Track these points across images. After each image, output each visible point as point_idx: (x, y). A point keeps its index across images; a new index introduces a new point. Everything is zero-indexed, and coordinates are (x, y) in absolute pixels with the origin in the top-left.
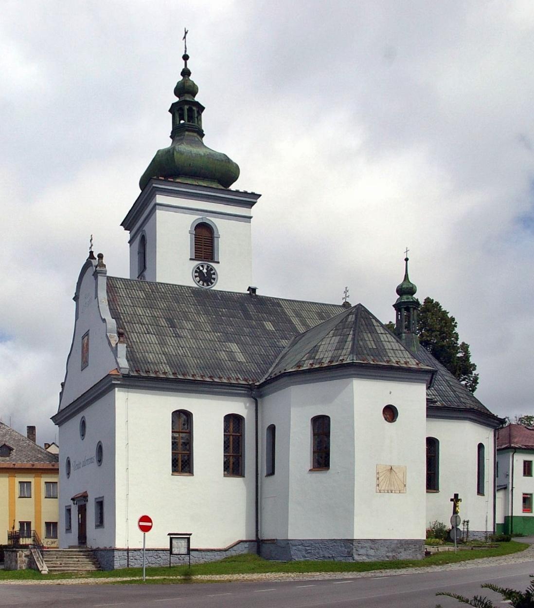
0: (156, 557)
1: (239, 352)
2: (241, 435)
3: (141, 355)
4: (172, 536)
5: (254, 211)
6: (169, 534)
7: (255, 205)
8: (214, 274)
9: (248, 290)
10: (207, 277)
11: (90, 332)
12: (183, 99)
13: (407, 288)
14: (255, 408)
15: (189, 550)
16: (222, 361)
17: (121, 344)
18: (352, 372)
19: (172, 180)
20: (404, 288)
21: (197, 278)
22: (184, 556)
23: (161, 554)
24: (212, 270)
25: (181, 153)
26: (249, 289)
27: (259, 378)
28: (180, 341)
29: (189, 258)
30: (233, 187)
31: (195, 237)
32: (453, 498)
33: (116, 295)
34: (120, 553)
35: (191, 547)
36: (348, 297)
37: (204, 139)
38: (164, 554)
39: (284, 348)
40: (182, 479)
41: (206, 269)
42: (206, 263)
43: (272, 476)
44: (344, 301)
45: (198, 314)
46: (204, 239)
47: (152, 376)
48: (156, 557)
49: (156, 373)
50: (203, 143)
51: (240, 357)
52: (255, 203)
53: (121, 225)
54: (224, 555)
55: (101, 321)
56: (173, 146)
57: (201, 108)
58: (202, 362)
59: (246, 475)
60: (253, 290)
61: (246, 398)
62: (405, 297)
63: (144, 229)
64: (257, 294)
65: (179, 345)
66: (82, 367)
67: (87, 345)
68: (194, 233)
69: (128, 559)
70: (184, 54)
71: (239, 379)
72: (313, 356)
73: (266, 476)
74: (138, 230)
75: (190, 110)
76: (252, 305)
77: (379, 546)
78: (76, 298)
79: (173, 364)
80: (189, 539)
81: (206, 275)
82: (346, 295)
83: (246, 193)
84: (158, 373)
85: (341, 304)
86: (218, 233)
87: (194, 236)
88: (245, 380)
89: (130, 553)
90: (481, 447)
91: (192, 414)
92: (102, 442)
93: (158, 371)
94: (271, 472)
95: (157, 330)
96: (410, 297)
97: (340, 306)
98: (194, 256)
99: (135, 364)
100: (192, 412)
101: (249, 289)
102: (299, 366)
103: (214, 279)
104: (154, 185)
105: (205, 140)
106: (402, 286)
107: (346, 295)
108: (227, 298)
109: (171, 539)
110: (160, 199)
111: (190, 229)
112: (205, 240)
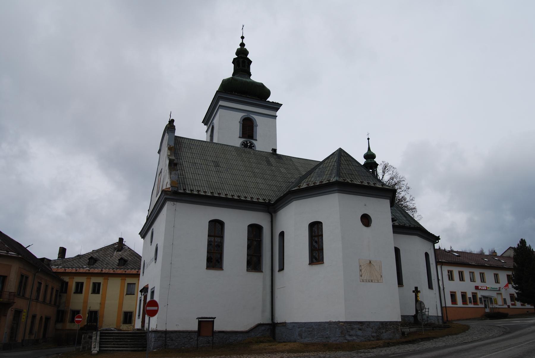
2: (261, 240)
4: (200, 320)
5: (278, 113)
8: (254, 146)
9: (272, 150)
13: (370, 155)
24: (252, 144)
29: (239, 136)
33: (182, 146)
39: (293, 183)
40: (214, 273)
42: (249, 140)
43: (283, 271)
53: (202, 123)
62: (369, 160)
68: (242, 123)
70: (242, 36)
71: (259, 199)
73: (279, 271)
74: (211, 123)
79: (212, 187)
84: (200, 192)
86: (257, 123)
87: (242, 125)
90: (427, 255)
93: (200, 191)
96: (372, 160)
98: (242, 135)
111: (239, 120)
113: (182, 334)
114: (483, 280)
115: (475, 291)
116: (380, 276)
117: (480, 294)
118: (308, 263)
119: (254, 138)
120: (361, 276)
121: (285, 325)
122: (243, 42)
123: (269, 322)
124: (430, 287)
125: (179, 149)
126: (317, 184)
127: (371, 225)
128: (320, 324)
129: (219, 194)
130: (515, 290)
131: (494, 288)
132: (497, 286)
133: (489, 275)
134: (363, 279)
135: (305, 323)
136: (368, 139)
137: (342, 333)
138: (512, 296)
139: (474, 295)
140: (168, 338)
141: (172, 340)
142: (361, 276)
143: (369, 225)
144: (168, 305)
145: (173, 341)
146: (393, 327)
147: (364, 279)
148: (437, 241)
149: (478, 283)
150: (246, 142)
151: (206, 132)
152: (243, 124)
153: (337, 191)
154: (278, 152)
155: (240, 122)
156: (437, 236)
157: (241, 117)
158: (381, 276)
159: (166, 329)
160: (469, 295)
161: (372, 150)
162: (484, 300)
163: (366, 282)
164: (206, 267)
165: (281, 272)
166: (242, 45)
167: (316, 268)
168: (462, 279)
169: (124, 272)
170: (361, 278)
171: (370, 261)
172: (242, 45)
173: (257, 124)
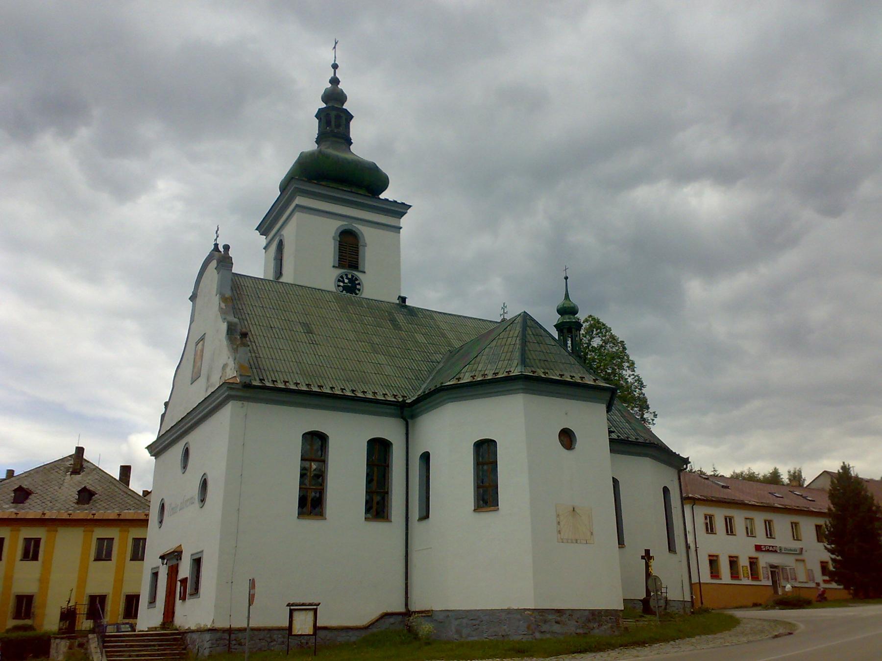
3: (268, 362)
4: (292, 607)
5: (404, 221)
6: (289, 605)
7: (406, 215)
8: (359, 284)
9: (398, 299)
10: (352, 287)
11: (206, 335)
12: (330, 104)
15: (316, 628)
20: (565, 307)
22: (308, 637)
24: (356, 279)
29: (332, 265)
30: (382, 196)
37: (351, 147)
39: (439, 363)
42: (352, 273)
43: (427, 520)
44: (502, 317)
46: (349, 246)
47: (280, 386)
49: (285, 384)
50: (350, 149)
52: (406, 213)
54: (364, 634)
56: (319, 148)
61: (393, 419)
62: (567, 316)
64: (407, 304)
65: (316, 354)
67: (202, 351)
69: (230, 643)
71: (386, 394)
73: (418, 520)
74: (275, 235)
75: (338, 117)
76: (401, 315)
77: (567, 620)
78: (193, 298)
80: (315, 611)
82: (504, 311)
87: (338, 243)
88: (395, 396)
89: (232, 635)
90: (666, 491)
93: (288, 382)
96: (572, 317)
98: (337, 263)
103: (359, 290)
107: (504, 311)
108: (374, 306)
109: (291, 611)
113: (256, 633)
114: (770, 534)
115: (755, 554)
116: (589, 534)
117: (765, 560)
118: (473, 509)
119: (360, 268)
120: (559, 532)
121: (431, 615)
122: (337, 75)
123: (402, 609)
124: (671, 548)
126: (489, 378)
127: (576, 447)
128: (493, 612)
129: (320, 387)
130: (829, 554)
131: (791, 550)
132: (796, 545)
133: (782, 524)
134: (562, 538)
135: (468, 611)
136: (566, 278)
137: (528, 627)
138: (824, 566)
139: (753, 562)
140: (233, 641)
141: (240, 644)
142: (559, 532)
143: (572, 447)
144: (232, 582)
145: (242, 645)
146: (610, 619)
147: (564, 538)
148: (685, 466)
149: (761, 539)
150: (346, 275)
151: (264, 248)
152: (339, 242)
153: (521, 391)
155: (334, 238)
156: (686, 457)
157: (337, 229)
158: (592, 533)
159: (230, 626)
160: (744, 562)
161: (575, 300)
162: (771, 571)
163: (568, 542)
164: (297, 515)
165: (424, 522)
166: (335, 81)
167: (487, 517)
168: (730, 530)
169: (90, 517)
170: (559, 535)
171: (574, 508)
172: (335, 81)
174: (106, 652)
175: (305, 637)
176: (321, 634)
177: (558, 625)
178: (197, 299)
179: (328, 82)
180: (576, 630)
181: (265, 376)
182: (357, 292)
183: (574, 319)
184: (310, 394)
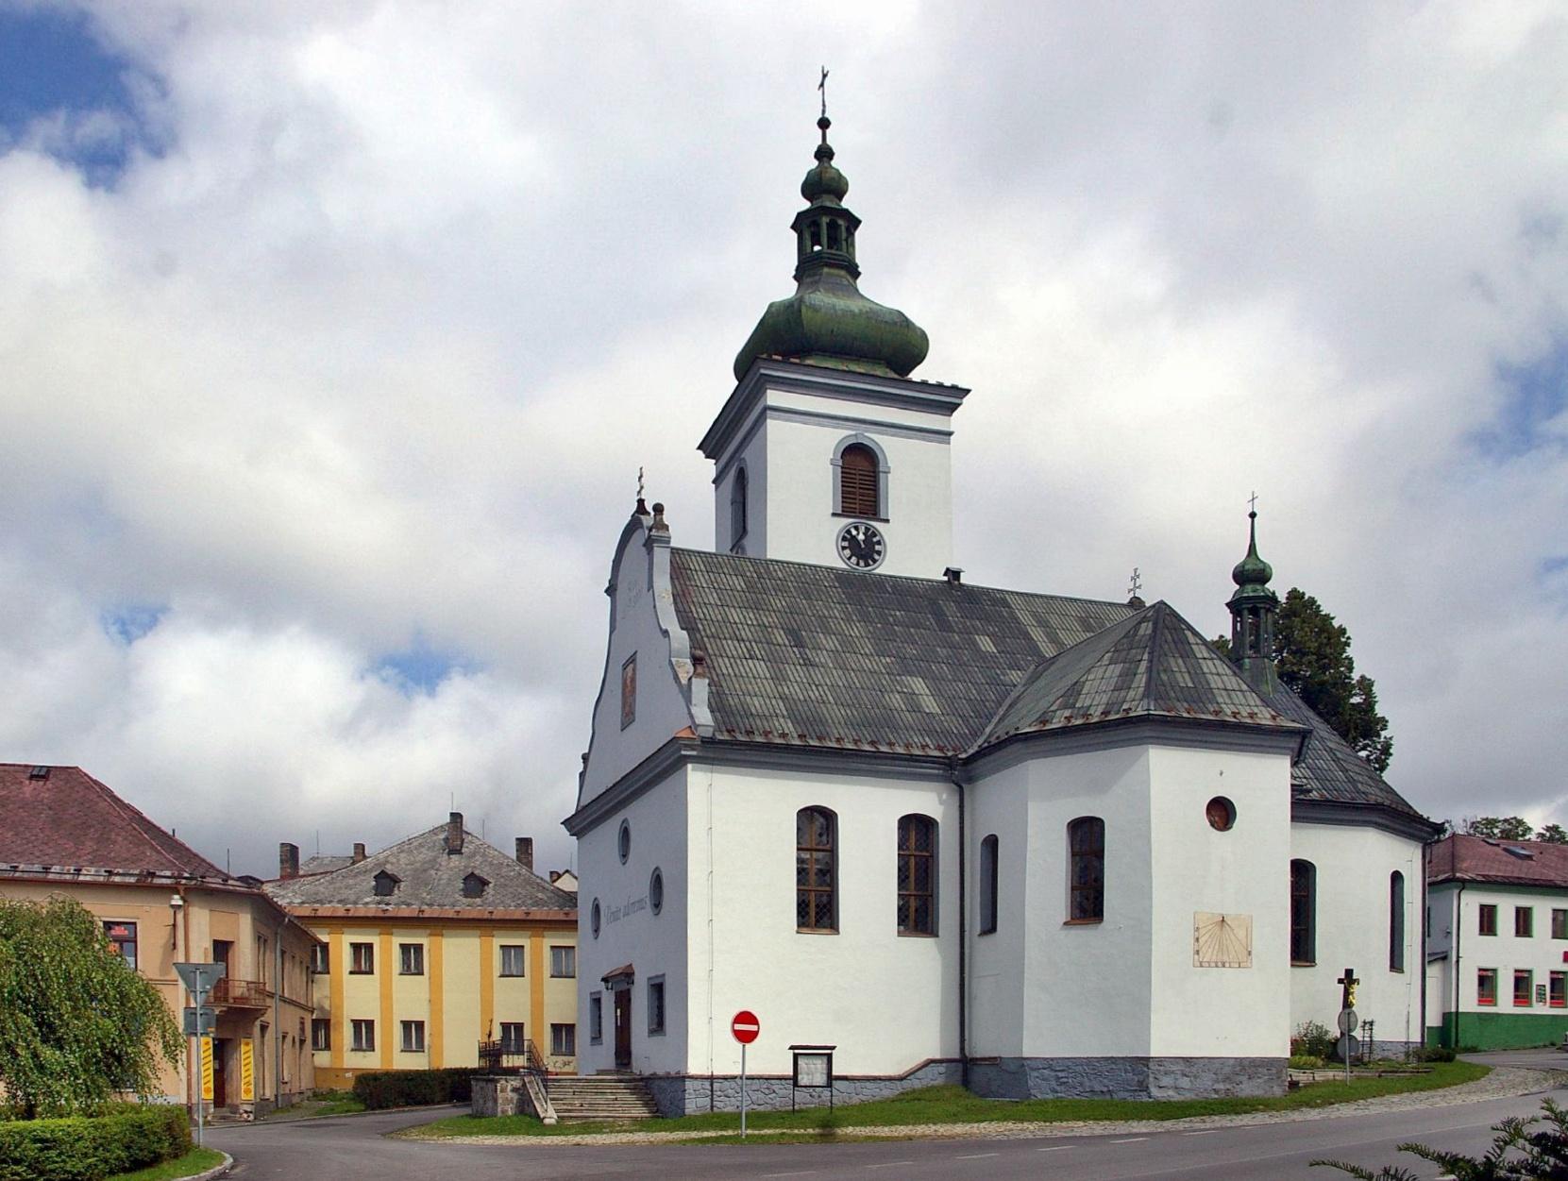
0: (767, 1091)
1: (927, 695)
2: (932, 856)
3: (737, 701)
4: (797, 1051)
5: (956, 421)
6: (792, 1048)
7: (960, 409)
8: (879, 543)
9: (945, 574)
10: (865, 549)
11: (638, 655)
12: (818, 203)
13: (1254, 570)
14: (958, 804)
15: (831, 1078)
16: (895, 712)
17: (698, 679)
18: (1148, 734)
19: (797, 361)
20: (1248, 570)
21: (845, 552)
22: (821, 1089)
23: (776, 1085)
24: (874, 535)
25: (815, 309)
26: (947, 572)
27: (967, 744)
28: (812, 673)
29: (831, 511)
30: (916, 375)
31: (842, 472)
32: (1343, 977)
33: (688, 583)
34: (697, 1084)
35: (835, 1073)
36: (1139, 587)
37: (858, 281)
38: (782, 1087)
39: (1015, 686)
40: (817, 941)
41: (864, 534)
44: (1131, 595)
45: (848, 620)
46: (860, 475)
47: (758, 740)
48: (767, 1091)
49: (766, 736)
50: (857, 290)
51: (930, 704)
52: (959, 405)
53: (699, 448)
54: (898, 1088)
55: (660, 634)
56: (799, 295)
57: (854, 222)
58: (856, 713)
59: (940, 934)
60: (954, 574)
61: (941, 784)
63: (742, 456)
64: (962, 581)
65: (811, 682)
66: (623, 724)
67: (633, 680)
68: (841, 464)
69: (712, 1095)
70: (820, 116)
71: (928, 746)
72: (1071, 701)
73: (980, 935)
74: (732, 458)
75: (833, 226)
76: (952, 604)
77: (1200, 1071)
78: (611, 591)
79: (799, 718)
80: (829, 1057)
81: (863, 546)
82: (1135, 584)
83: (940, 386)
84: (770, 736)
85: (1126, 601)
86: (887, 463)
87: (840, 469)
88: (940, 748)
89: (715, 1085)
90: (1397, 878)
91: (836, 814)
92: (662, 869)
93: (770, 732)
94: (990, 927)
95: (768, 651)
96: (1259, 587)
97: (1123, 605)
98: (840, 508)
99: (726, 719)
100: (836, 811)
101: (947, 572)
102: (1044, 722)
103: (879, 553)
104: (763, 371)
105: (861, 284)
106: (1243, 567)
107: (1135, 584)
108: (904, 590)
109: (796, 1056)
110: (774, 397)
112: (861, 477)
125: (684, 595)
152: (842, 468)
154: (964, 579)
161: (1262, 553)
173: (889, 465)
174: (551, 1099)
175: (817, 1089)
176: (836, 1084)
177: (1185, 1078)
178: (618, 592)
179: (813, 156)
180: (1213, 1085)
181: (735, 725)
182: (876, 557)
183: (1263, 591)
184: (806, 750)
